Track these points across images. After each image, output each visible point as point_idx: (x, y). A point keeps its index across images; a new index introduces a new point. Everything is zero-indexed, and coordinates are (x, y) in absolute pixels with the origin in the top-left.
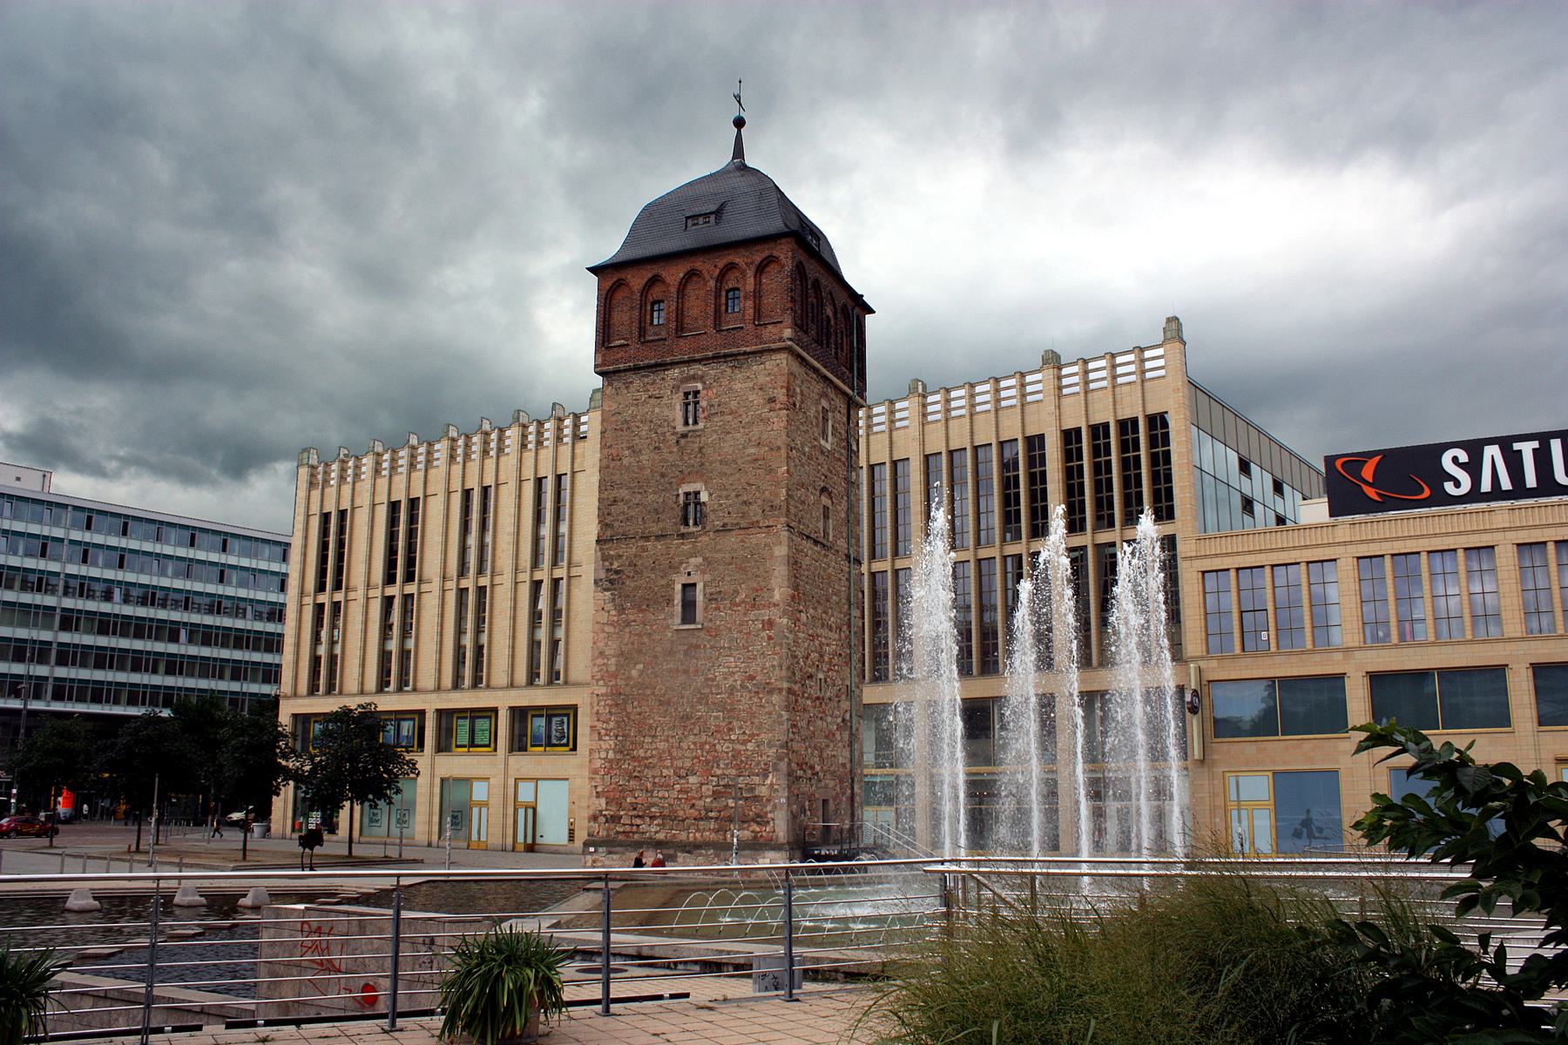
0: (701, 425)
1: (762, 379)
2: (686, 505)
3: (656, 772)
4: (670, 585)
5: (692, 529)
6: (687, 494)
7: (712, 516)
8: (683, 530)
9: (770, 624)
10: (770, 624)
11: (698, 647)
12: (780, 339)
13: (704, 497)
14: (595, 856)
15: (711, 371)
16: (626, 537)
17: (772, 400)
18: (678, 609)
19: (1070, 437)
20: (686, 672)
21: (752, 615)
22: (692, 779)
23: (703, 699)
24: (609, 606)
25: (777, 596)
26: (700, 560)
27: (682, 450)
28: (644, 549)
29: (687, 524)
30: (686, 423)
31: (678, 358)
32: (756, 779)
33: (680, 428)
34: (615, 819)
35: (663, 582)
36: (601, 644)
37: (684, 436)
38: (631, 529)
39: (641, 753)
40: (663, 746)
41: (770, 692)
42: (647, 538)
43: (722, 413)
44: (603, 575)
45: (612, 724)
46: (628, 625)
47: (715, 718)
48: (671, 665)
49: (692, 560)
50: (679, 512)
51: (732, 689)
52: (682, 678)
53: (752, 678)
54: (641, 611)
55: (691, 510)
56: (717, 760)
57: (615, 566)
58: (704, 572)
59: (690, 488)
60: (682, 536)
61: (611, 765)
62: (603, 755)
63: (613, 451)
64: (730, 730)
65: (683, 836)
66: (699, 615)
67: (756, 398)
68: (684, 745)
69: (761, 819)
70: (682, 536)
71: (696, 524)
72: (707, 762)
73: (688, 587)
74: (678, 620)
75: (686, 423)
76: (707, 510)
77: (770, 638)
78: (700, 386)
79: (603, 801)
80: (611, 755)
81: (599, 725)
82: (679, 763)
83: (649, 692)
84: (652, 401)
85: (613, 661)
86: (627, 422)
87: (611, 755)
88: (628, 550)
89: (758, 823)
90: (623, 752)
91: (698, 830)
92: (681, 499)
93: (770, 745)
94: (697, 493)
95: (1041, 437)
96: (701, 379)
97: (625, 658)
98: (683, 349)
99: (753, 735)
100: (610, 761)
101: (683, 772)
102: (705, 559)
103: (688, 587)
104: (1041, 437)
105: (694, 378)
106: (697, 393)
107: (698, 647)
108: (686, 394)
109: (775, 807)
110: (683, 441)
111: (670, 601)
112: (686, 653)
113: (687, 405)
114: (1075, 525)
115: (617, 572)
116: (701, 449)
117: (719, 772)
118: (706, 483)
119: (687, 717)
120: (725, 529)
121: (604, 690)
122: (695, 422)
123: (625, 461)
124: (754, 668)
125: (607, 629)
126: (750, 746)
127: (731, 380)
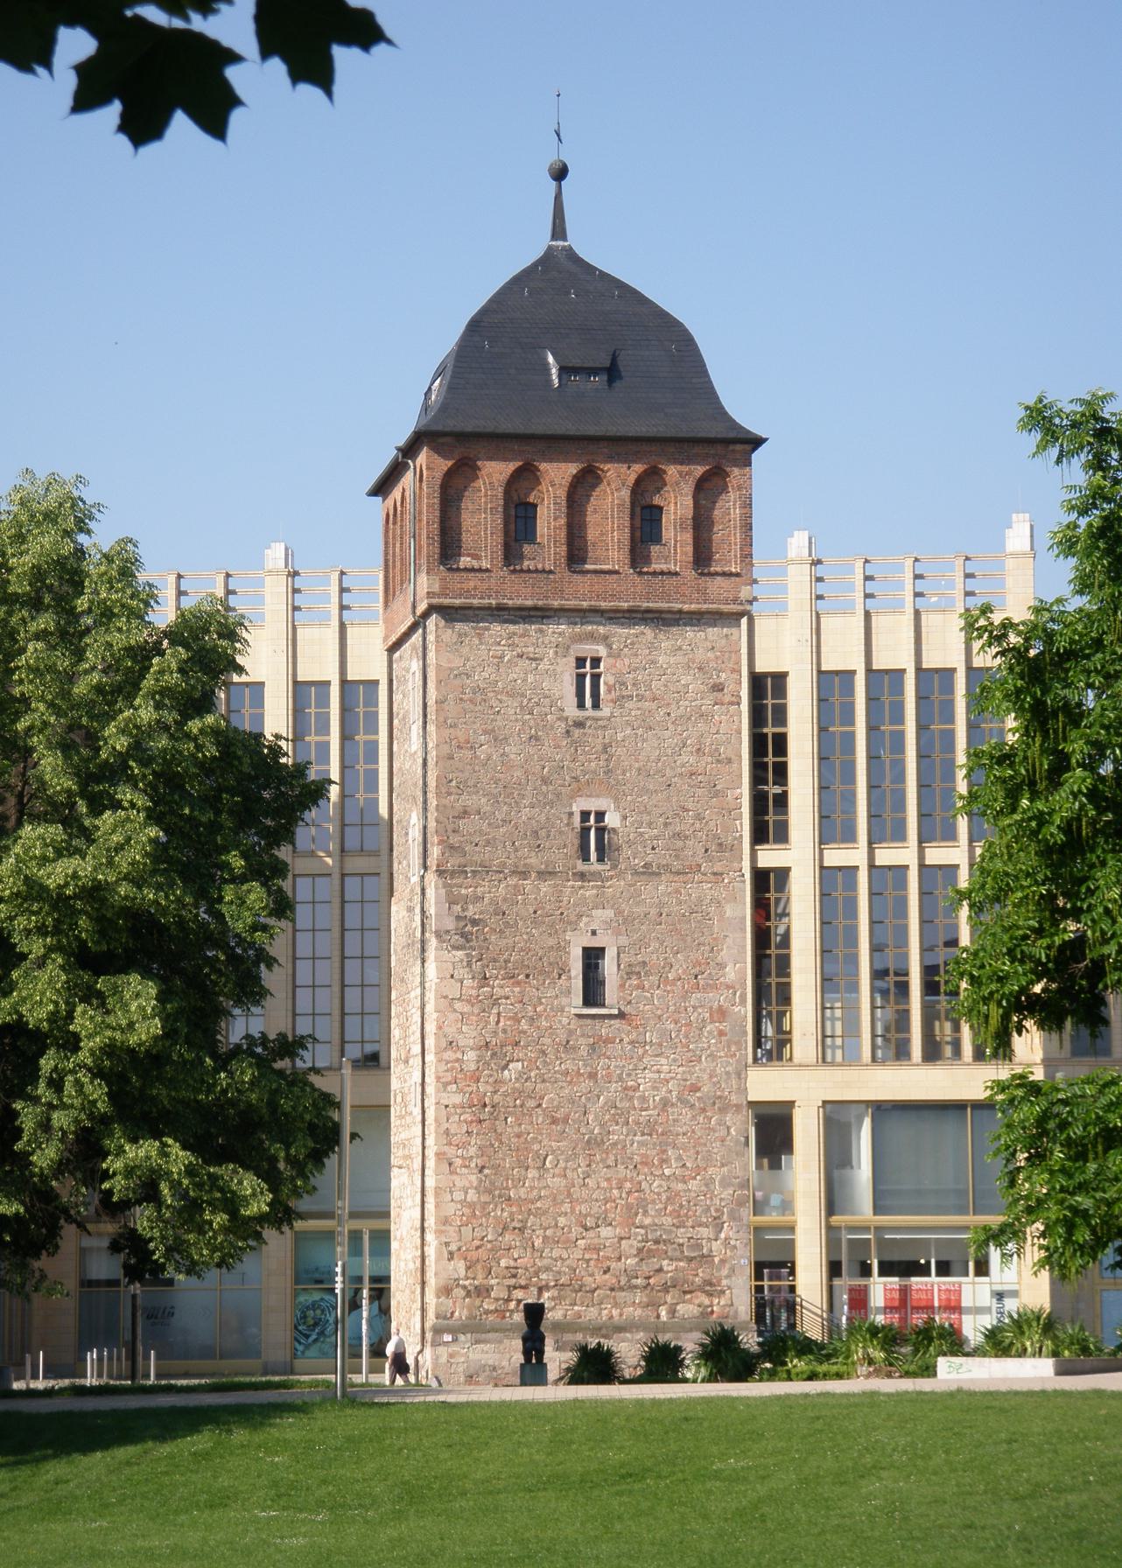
0: (606, 711)
1: (700, 655)
2: (585, 832)
3: (546, 1221)
4: (562, 948)
5: (597, 867)
6: (585, 815)
7: (627, 852)
8: (581, 866)
9: (722, 1014)
10: (722, 1014)
11: (609, 1041)
12: (735, 601)
13: (612, 820)
14: (454, 1348)
15: (621, 633)
16: (484, 870)
17: (718, 688)
18: (578, 984)
19: (832, 685)
20: (593, 1076)
21: (695, 998)
22: (605, 1232)
23: (621, 1116)
24: (461, 972)
25: (730, 974)
26: (609, 913)
27: (576, 744)
28: (517, 890)
29: (586, 858)
30: (581, 705)
31: (572, 603)
32: (705, 1232)
33: (572, 711)
34: (482, 1292)
35: (551, 942)
36: (450, 1031)
37: (580, 724)
38: (498, 857)
39: (522, 1192)
40: (558, 1182)
41: (723, 1110)
42: (524, 875)
43: (641, 698)
44: (450, 924)
45: (472, 1151)
46: (496, 1003)
47: (638, 1146)
48: (569, 1065)
49: (597, 913)
50: (573, 840)
51: (665, 1103)
52: (586, 1084)
53: (695, 1089)
54: (518, 983)
55: (594, 839)
56: (643, 1205)
57: (471, 911)
58: (618, 933)
59: (592, 805)
60: (582, 876)
61: (473, 1213)
62: (459, 1196)
63: (461, 735)
64: (663, 1161)
65: (592, 1313)
66: (611, 992)
67: (694, 683)
68: (591, 1182)
69: (711, 1288)
70: (582, 876)
71: (600, 859)
72: (629, 1207)
73: (593, 957)
74: (578, 999)
75: (581, 705)
76: (620, 840)
77: (721, 1033)
78: (602, 651)
79: (461, 1266)
80: (472, 1196)
81: (451, 1151)
82: (584, 1208)
83: (531, 1103)
84: (520, 662)
85: (471, 1056)
86: (483, 691)
87: (472, 1196)
88: (495, 891)
89: (710, 1294)
90: (494, 1191)
91: (616, 1305)
92: (577, 819)
93: (725, 1183)
94: (600, 816)
95: (780, 679)
96: (605, 639)
97: (495, 1053)
98: (580, 591)
99: (698, 1170)
100: (472, 1205)
101: (590, 1222)
102: (619, 912)
103: (593, 957)
104: (780, 679)
105: (592, 637)
106: (596, 662)
107: (609, 1041)
108: (580, 662)
109: (733, 1270)
110: (577, 732)
111: (563, 971)
112: (593, 1047)
113: (581, 678)
114: (833, 827)
115: (474, 922)
116: (605, 748)
117: (647, 1221)
118: (616, 800)
119: (593, 1143)
120: (648, 872)
121: (457, 1099)
122: (596, 705)
123: (482, 753)
124: (701, 1071)
125: (458, 1005)
126: (693, 1185)
127: (651, 647)
